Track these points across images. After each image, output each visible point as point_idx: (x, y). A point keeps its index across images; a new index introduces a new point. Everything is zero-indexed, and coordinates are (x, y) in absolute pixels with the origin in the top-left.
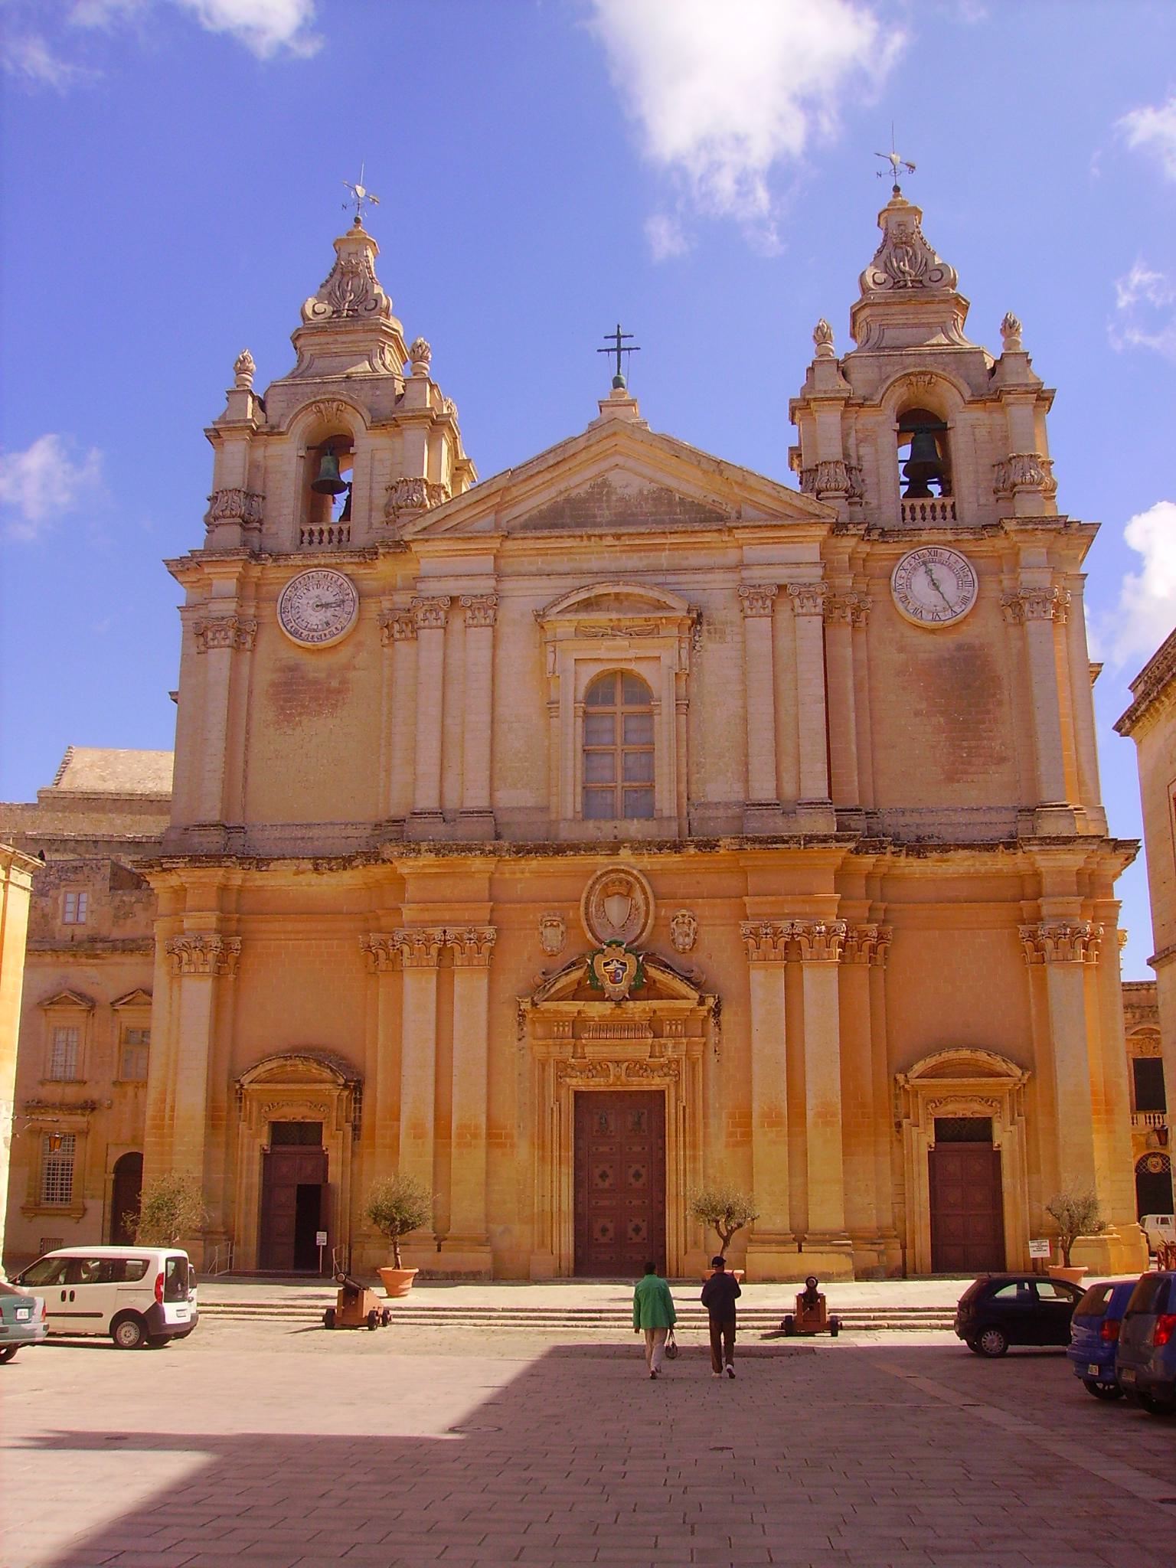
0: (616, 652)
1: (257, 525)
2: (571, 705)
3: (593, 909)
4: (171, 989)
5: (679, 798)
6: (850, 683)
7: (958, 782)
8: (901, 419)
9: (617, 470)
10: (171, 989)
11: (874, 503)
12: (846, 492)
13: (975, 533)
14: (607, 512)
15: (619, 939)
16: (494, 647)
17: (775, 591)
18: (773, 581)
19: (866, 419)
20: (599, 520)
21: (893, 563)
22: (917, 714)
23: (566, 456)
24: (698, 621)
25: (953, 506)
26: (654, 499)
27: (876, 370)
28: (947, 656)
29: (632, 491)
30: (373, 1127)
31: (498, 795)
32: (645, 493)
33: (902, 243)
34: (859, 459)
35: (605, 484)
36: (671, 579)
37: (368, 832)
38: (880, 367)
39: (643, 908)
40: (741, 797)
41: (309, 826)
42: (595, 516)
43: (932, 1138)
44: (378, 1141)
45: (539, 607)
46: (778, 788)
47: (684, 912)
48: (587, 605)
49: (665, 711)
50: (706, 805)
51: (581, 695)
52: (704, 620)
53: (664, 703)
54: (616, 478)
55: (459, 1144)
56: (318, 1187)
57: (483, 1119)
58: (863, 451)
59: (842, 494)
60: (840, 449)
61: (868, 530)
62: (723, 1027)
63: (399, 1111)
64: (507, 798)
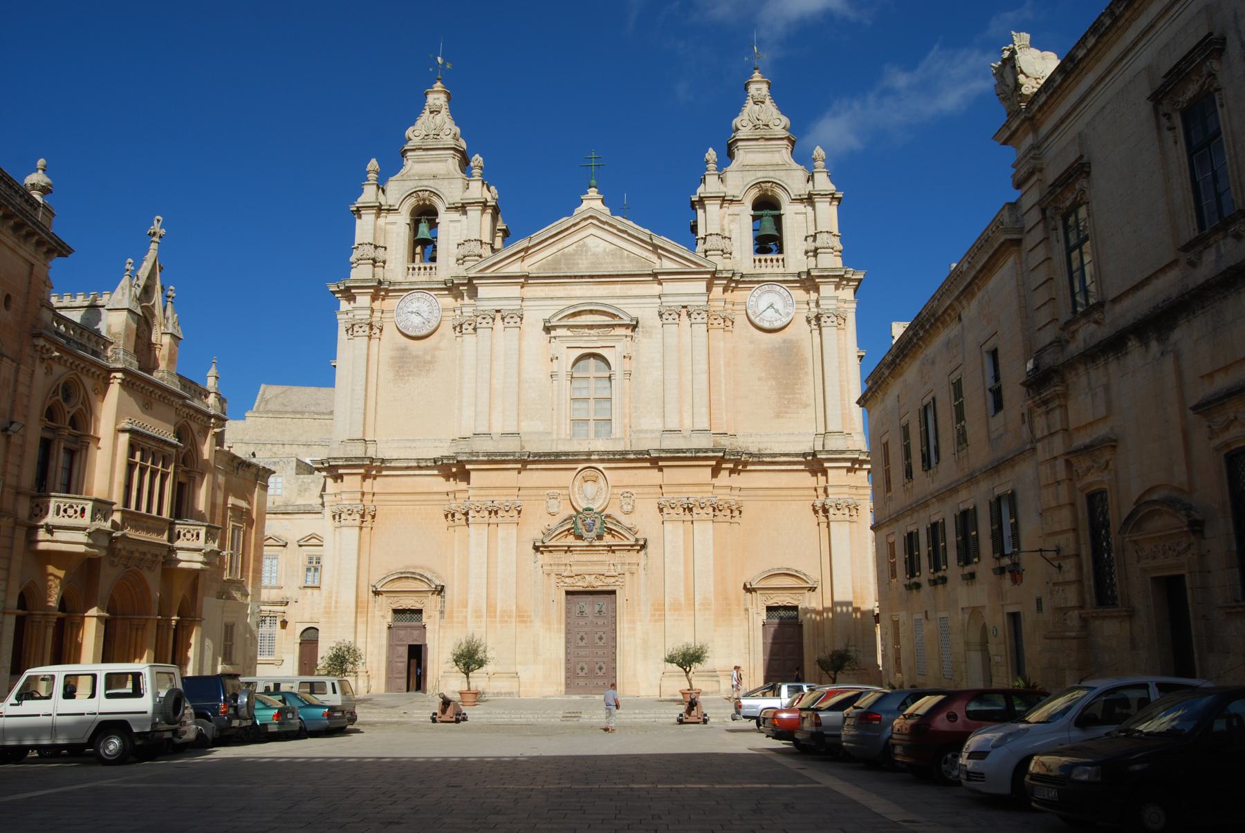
0: (591, 342)
1: (382, 264)
2: (564, 373)
3: (576, 489)
4: (335, 534)
5: (625, 426)
6: (722, 362)
7: (782, 418)
8: (755, 207)
9: (592, 237)
10: (335, 534)
11: (738, 257)
12: (722, 251)
13: (794, 276)
14: (585, 262)
15: (591, 506)
16: (520, 339)
17: (680, 309)
18: (679, 304)
19: (734, 208)
20: (581, 266)
21: (748, 292)
22: (760, 379)
23: (563, 228)
24: (634, 327)
25: (783, 260)
26: (613, 254)
27: (741, 179)
28: (777, 346)
29: (599, 250)
30: (452, 612)
31: (523, 424)
32: (607, 250)
34: (730, 231)
35: (584, 245)
36: (622, 301)
37: (449, 444)
38: (743, 178)
39: (604, 489)
40: (661, 427)
41: (414, 440)
42: (578, 264)
43: (764, 617)
44: (455, 619)
45: (547, 317)
46: (681, 421)
47: (627, 490)
48: (574, 315)
49: (617, 377)
50: (641, 431)
51: (569, 369)
52: (639, 325)
53: (617, 373)
54: (591, 242)
55: (501, 622)
56: (420, 646)
57: (514, 607)
58: (732, 227)
59: (720, 252)
60: (719, 227)
61: (734, 274)
62: (649, 555)
63: (467, 602)
64: (526, 426)
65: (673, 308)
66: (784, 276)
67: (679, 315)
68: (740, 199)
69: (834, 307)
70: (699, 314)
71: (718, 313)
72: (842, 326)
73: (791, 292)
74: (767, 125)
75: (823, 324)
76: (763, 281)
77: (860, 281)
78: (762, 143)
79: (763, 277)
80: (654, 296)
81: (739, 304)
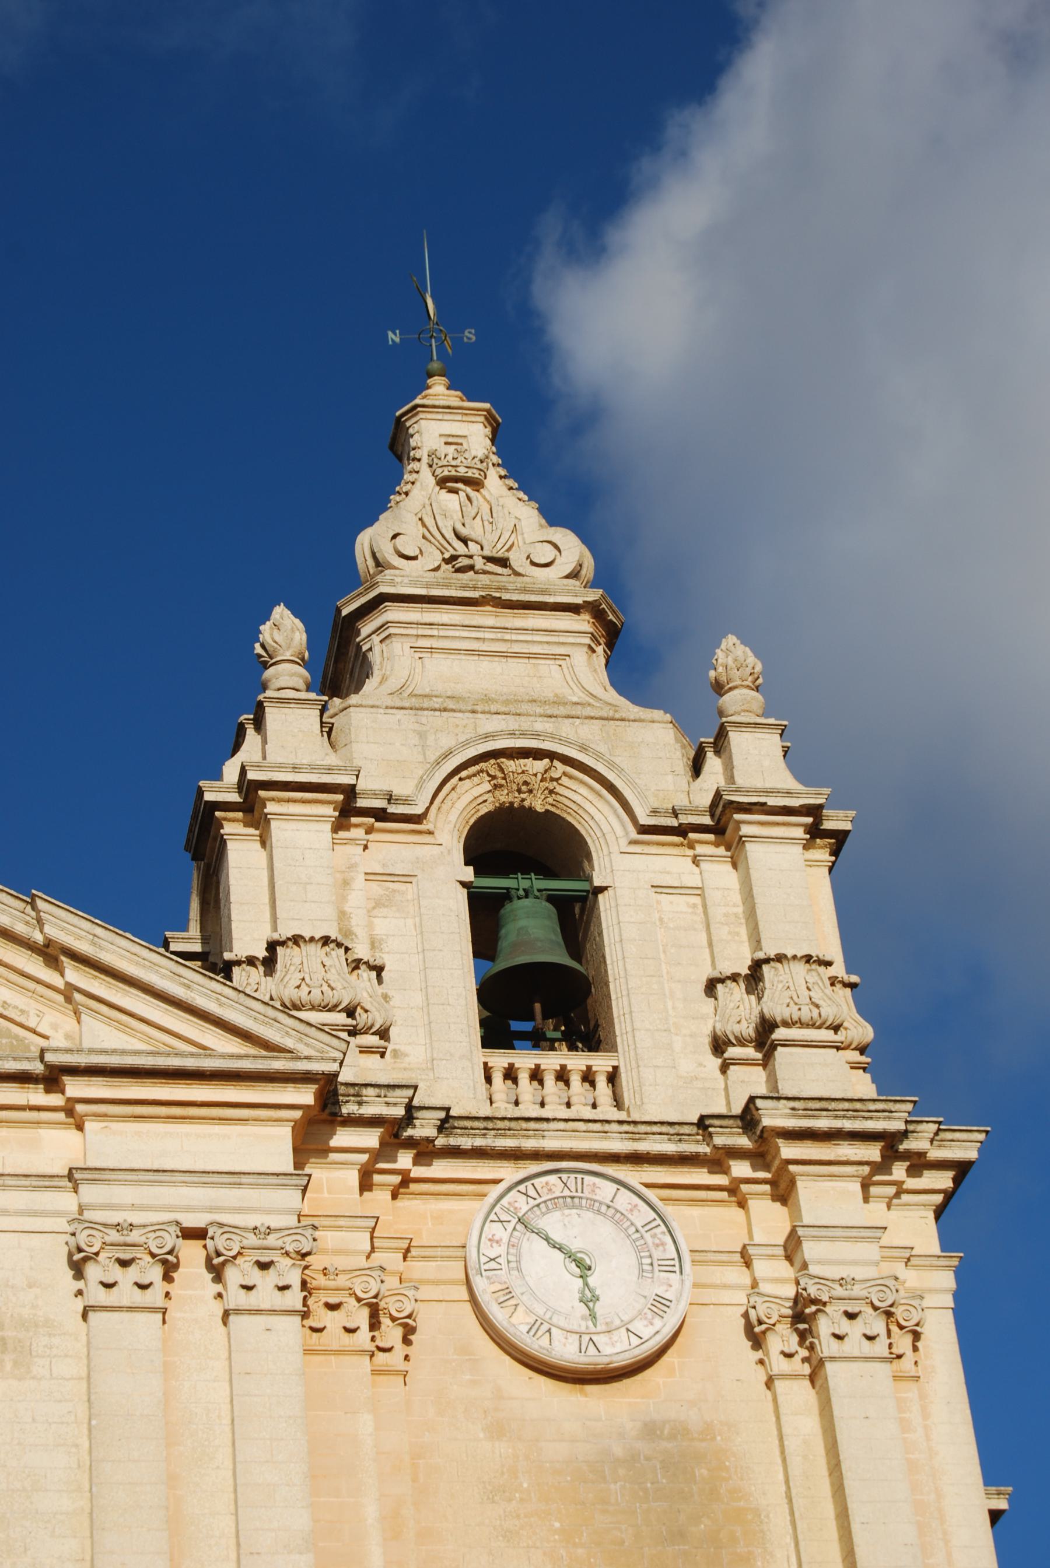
12: (350, 1012)
33: (456, 480)
65: (135, 1236)
66: (634, 1137)
67: (169, 1270)
68: (419, 810)
69: (871, 1272)
70: (264, 1266)
71: (342, 1281)
72: (906, 1365)
73: (669, 1211)
74: (503, 562)
75: (827, 1346)
76: (537, 1156)
77: (962, 1169)
78: (486, 617)
79: (540, 1134)
80: (44, 1180)
81: (433, 1252)
